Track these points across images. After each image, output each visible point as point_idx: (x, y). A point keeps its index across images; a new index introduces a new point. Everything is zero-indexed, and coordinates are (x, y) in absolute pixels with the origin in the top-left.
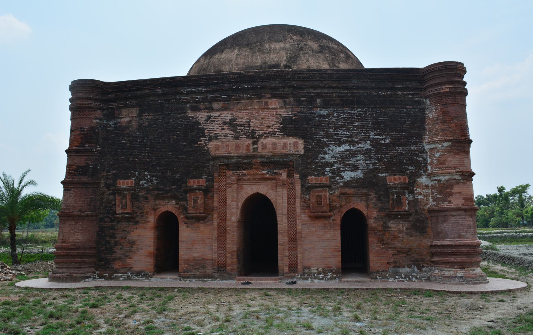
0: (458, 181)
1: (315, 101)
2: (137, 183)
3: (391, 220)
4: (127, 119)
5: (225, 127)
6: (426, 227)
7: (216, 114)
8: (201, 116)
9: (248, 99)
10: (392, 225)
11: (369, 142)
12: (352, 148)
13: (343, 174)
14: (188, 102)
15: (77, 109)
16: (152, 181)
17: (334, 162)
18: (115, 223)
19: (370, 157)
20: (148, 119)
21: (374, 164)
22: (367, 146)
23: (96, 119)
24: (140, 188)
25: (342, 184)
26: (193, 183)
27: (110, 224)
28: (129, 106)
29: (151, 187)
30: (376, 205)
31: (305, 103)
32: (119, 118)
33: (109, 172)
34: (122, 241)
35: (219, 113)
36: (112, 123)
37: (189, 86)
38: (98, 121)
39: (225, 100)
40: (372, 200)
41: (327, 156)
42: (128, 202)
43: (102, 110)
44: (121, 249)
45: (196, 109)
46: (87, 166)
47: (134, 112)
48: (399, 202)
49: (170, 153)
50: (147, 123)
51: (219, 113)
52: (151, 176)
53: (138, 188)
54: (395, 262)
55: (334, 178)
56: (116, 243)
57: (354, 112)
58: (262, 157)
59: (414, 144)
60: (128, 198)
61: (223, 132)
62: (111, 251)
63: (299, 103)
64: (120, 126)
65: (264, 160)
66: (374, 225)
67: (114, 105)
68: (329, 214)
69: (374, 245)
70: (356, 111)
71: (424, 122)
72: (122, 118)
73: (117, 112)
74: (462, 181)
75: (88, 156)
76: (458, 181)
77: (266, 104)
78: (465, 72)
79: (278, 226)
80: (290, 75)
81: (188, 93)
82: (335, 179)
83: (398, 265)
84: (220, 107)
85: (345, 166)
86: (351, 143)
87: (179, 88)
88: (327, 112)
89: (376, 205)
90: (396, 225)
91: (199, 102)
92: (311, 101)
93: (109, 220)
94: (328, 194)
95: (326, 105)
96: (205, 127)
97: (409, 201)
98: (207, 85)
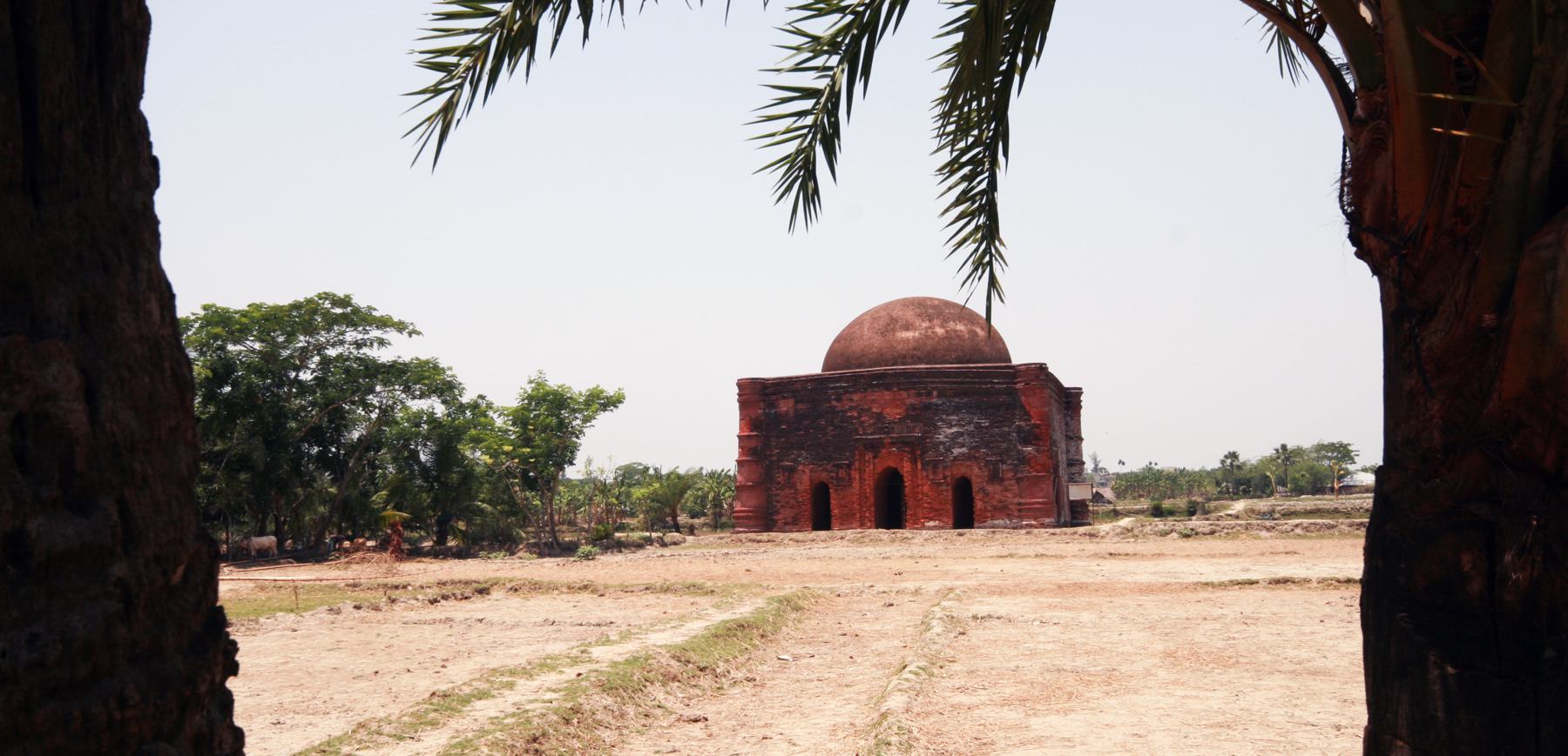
15: (744, 403)
47: (791, 403)
92: (929, 394)
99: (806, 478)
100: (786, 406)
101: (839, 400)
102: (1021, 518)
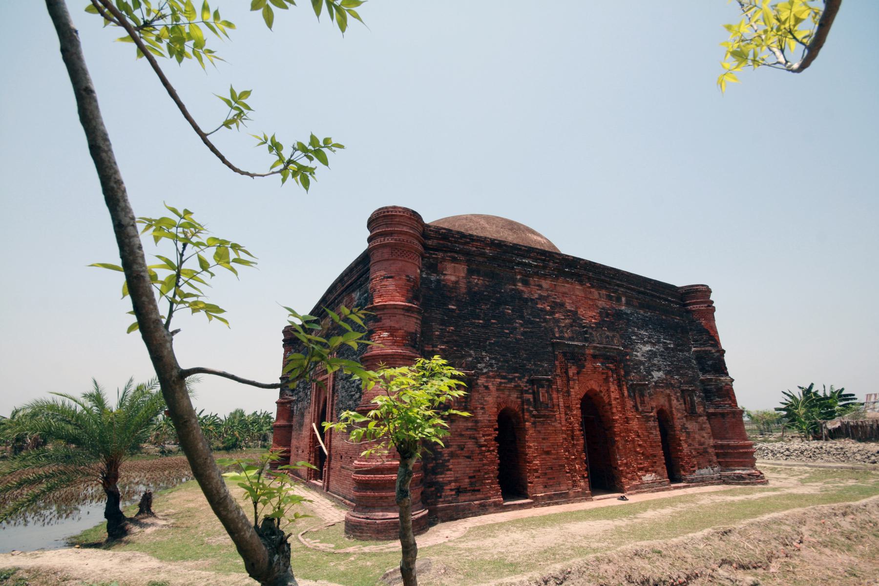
4: (453, 278)
20: (477, 284)
21: (669, 366)
52: (490, 358)
63: (609, 298)
67: (440, 255)
72: (445, 275)
92: (618, 300)
99: (490, 399)
100: (454, 274)
101: (526, 283)
102: (725, 466)
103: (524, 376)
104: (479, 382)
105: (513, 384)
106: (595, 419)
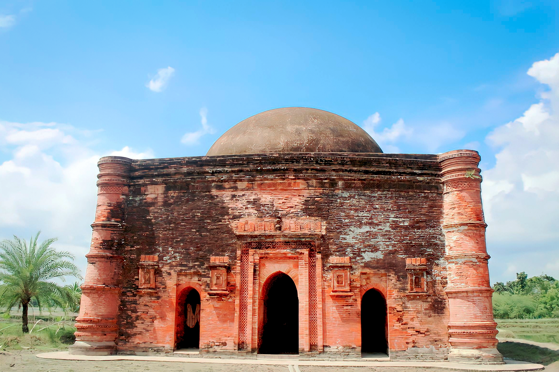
0: (474, 264)
1: (336, 184)
2: (161, 258)
3: (409, 300)
4: (153, 196)
5: (249, 206)
6: (444, 308)
7: (241, 193)
8: (226, 196)
9: (272, 180)
10: (410, 305)
11: (388, 224)
12: (372, 229)
13: (363, 254)
14: (213, 181)
16: (175, 257)
17: (355, 243)
18: (137, 298)
19: (389, 239)
21: (394, 246)
22: (387, 227)
23: (123, 195)
24: (163, 264)
25: (363, 265)
26: (215, 260)
27: (132, 298)
28: (156, 184)
29: (174, 263)
30: (395, 285)
31: (327, 185)
32: (145, 194)
33: (133, 247)
34: (143, 316)
35: (243, 193)
36: (137, 199)
37: (215, 166)
38: (124, 197)
39: (249, 180)
40: (391, 280)
41: (347, 237)
42: (152, 277)
43: (129, 186)
44: (142, 323)
45: (220, 188)
46: (112, 240)
47: (160, 189)
48: (417, 283)
49: (195, 230)
50: (172, 201)
51: (243, 193)
52: (175, 252)
53: (162, 263)
54: (414, 342)
55: (355, 258)
56: (137, 318)
57: (373, 195)
58: (285, 236)
59: (431, 227)
60: (152, 272)
61: (247, 211)
62: (131, 325)
63: (322, 185)
64: (146, 202)
65: (287, 239)
66: (393, 306)
67: (141, 181)
68: (350, 294)
69: (393, 325)
70: (376, 195)
71: (441, 206)
72: (147, 194)
73: (143, 189)
74: (478, 263)
75: (114, 231)
76: (474, 264)
77: (289, 185)
78: (480, 160)
79: (300, 305)
80: (313, 157)
81: (213, 173)
82: (355, 259)
83: (416, 345)
84: (244, 187)
85: (365, 247)
86: (371, 224)
87: (204, 167)
88: (348, 194)
89: (395, 285)
90: (415, 305)
91: (225, 181)
92: (333, 184)
93: (132, 294)
94: (349, 273)
95: (348, 187)
96: (229, 206)
97: (427, 283)
98: (232, 165)
103: (203, 264)
104: (163, 269)
105: (192, 271)
106: (280, 298)
